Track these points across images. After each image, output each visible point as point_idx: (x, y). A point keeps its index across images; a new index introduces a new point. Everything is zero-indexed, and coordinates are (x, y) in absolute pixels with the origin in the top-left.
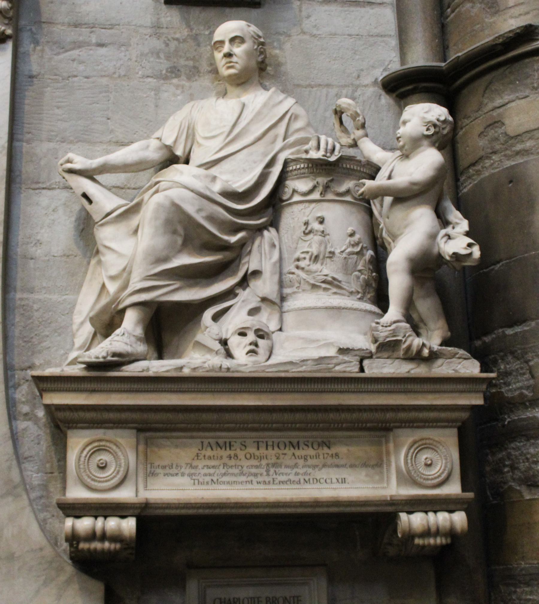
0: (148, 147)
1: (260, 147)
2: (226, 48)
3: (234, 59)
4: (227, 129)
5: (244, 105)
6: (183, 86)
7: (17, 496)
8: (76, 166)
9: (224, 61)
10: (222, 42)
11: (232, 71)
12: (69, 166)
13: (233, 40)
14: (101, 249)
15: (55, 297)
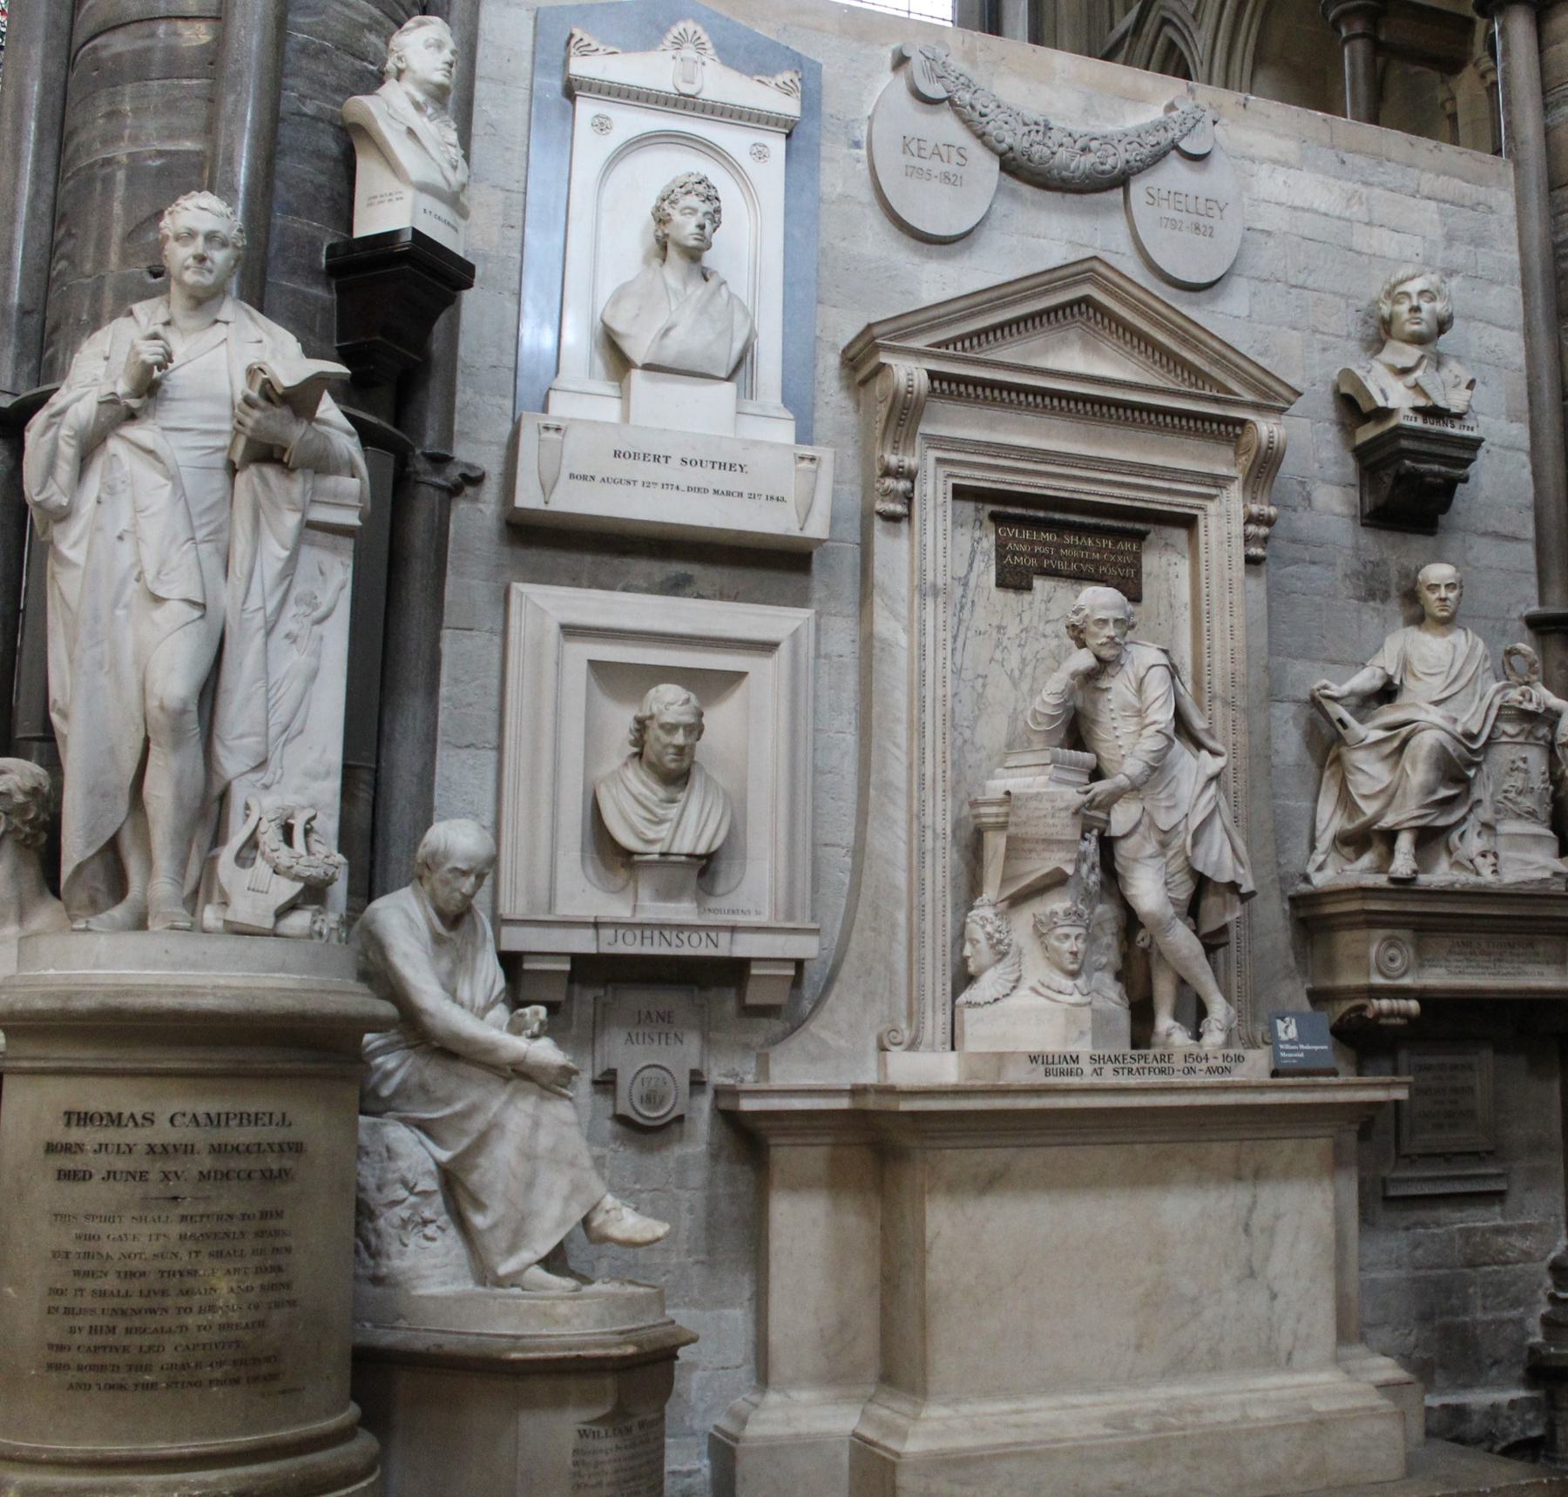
0: (1374, 676)
1: (1469, 689)
2: (1443, 593)
3: (1448, 603)
4: (1445, 669)
5: (1454, 647)
6: (1378, 610)
7: (1294, 978)
8: (1335, 694)
9: (1437, 603)
10: (1438, 586)
11: (1445, 614)
12: (1328, 692)
13: (1447, 586)
14: (1351, 768)
15: (1292, 803)
